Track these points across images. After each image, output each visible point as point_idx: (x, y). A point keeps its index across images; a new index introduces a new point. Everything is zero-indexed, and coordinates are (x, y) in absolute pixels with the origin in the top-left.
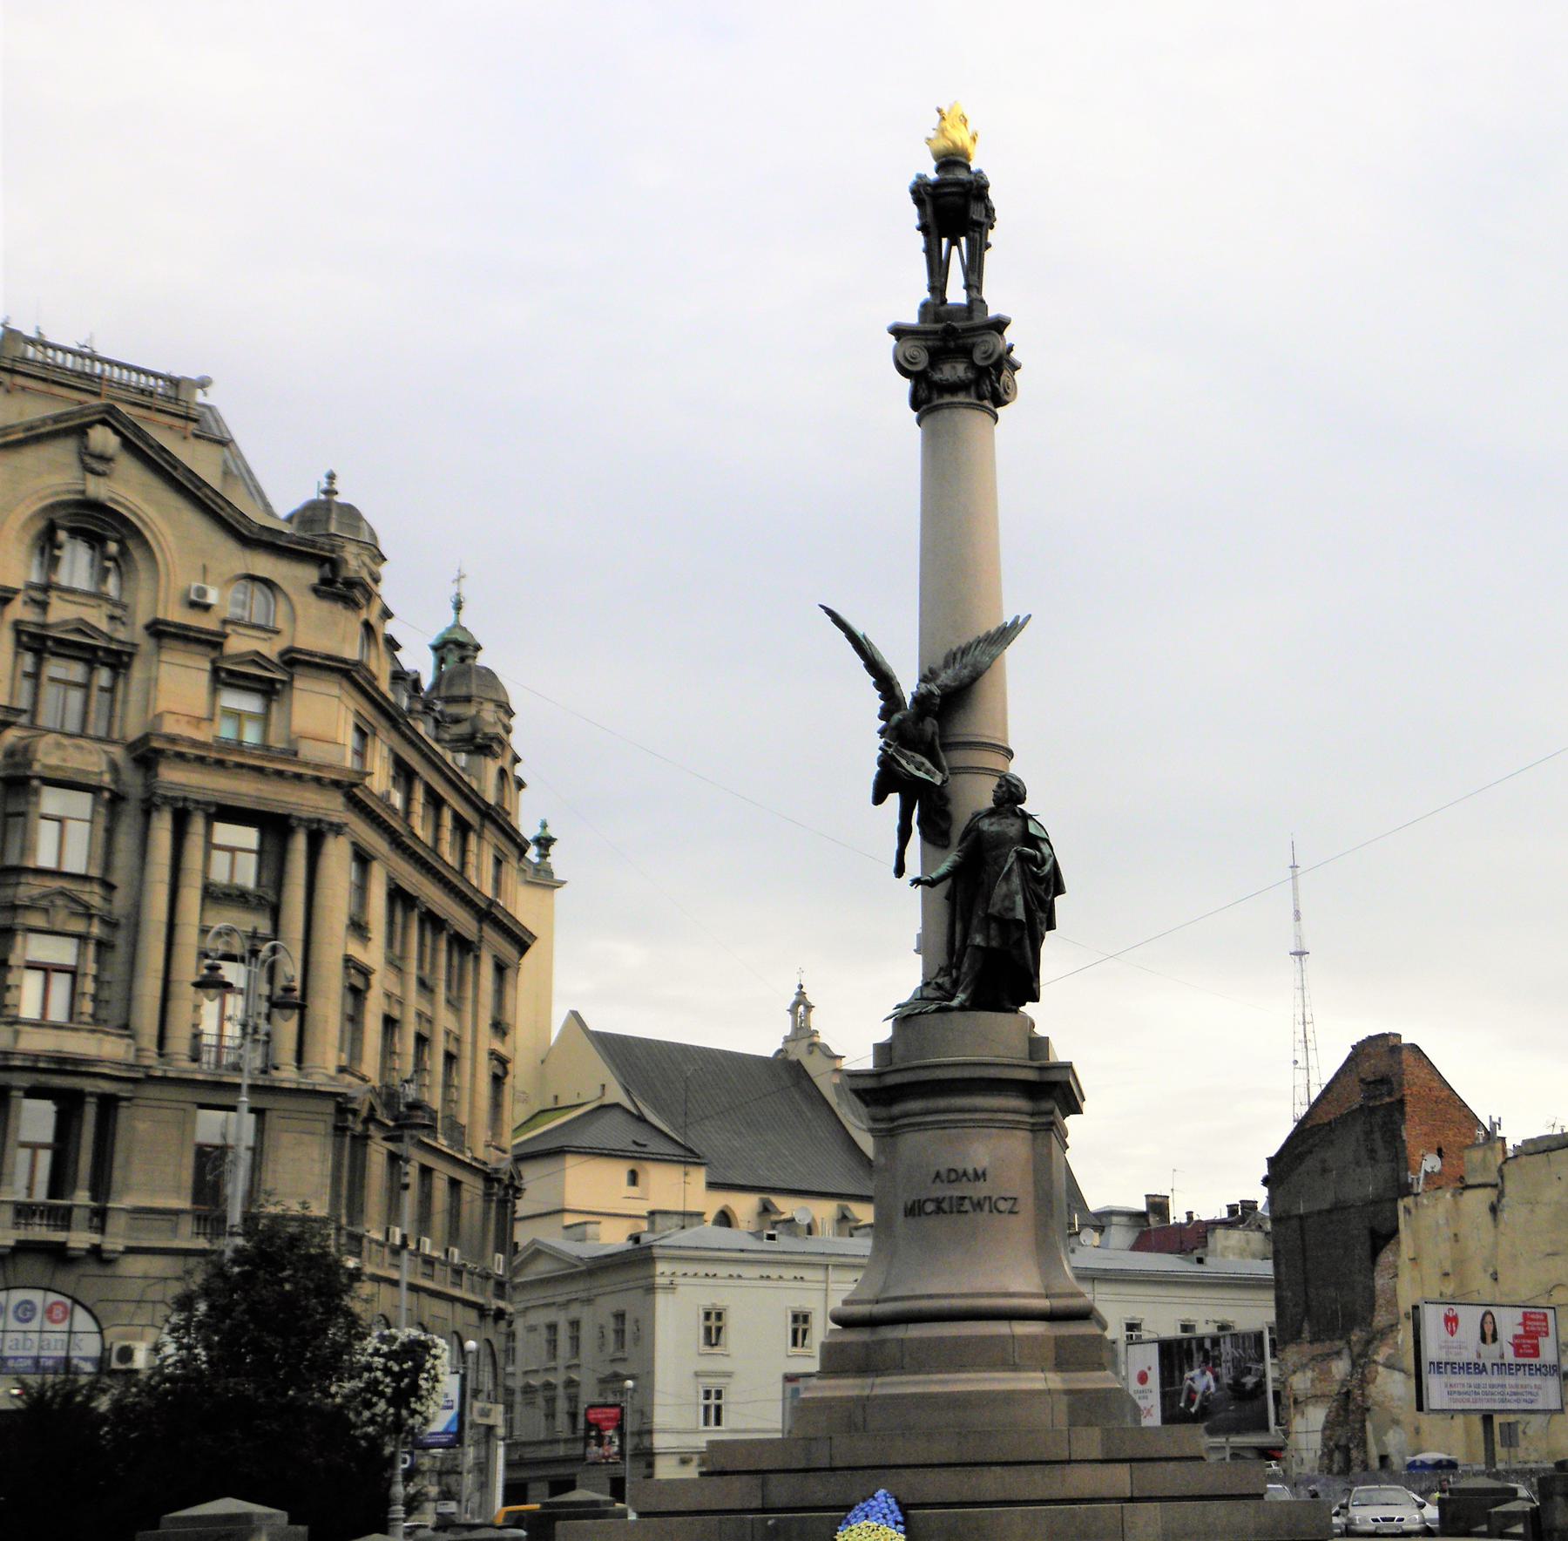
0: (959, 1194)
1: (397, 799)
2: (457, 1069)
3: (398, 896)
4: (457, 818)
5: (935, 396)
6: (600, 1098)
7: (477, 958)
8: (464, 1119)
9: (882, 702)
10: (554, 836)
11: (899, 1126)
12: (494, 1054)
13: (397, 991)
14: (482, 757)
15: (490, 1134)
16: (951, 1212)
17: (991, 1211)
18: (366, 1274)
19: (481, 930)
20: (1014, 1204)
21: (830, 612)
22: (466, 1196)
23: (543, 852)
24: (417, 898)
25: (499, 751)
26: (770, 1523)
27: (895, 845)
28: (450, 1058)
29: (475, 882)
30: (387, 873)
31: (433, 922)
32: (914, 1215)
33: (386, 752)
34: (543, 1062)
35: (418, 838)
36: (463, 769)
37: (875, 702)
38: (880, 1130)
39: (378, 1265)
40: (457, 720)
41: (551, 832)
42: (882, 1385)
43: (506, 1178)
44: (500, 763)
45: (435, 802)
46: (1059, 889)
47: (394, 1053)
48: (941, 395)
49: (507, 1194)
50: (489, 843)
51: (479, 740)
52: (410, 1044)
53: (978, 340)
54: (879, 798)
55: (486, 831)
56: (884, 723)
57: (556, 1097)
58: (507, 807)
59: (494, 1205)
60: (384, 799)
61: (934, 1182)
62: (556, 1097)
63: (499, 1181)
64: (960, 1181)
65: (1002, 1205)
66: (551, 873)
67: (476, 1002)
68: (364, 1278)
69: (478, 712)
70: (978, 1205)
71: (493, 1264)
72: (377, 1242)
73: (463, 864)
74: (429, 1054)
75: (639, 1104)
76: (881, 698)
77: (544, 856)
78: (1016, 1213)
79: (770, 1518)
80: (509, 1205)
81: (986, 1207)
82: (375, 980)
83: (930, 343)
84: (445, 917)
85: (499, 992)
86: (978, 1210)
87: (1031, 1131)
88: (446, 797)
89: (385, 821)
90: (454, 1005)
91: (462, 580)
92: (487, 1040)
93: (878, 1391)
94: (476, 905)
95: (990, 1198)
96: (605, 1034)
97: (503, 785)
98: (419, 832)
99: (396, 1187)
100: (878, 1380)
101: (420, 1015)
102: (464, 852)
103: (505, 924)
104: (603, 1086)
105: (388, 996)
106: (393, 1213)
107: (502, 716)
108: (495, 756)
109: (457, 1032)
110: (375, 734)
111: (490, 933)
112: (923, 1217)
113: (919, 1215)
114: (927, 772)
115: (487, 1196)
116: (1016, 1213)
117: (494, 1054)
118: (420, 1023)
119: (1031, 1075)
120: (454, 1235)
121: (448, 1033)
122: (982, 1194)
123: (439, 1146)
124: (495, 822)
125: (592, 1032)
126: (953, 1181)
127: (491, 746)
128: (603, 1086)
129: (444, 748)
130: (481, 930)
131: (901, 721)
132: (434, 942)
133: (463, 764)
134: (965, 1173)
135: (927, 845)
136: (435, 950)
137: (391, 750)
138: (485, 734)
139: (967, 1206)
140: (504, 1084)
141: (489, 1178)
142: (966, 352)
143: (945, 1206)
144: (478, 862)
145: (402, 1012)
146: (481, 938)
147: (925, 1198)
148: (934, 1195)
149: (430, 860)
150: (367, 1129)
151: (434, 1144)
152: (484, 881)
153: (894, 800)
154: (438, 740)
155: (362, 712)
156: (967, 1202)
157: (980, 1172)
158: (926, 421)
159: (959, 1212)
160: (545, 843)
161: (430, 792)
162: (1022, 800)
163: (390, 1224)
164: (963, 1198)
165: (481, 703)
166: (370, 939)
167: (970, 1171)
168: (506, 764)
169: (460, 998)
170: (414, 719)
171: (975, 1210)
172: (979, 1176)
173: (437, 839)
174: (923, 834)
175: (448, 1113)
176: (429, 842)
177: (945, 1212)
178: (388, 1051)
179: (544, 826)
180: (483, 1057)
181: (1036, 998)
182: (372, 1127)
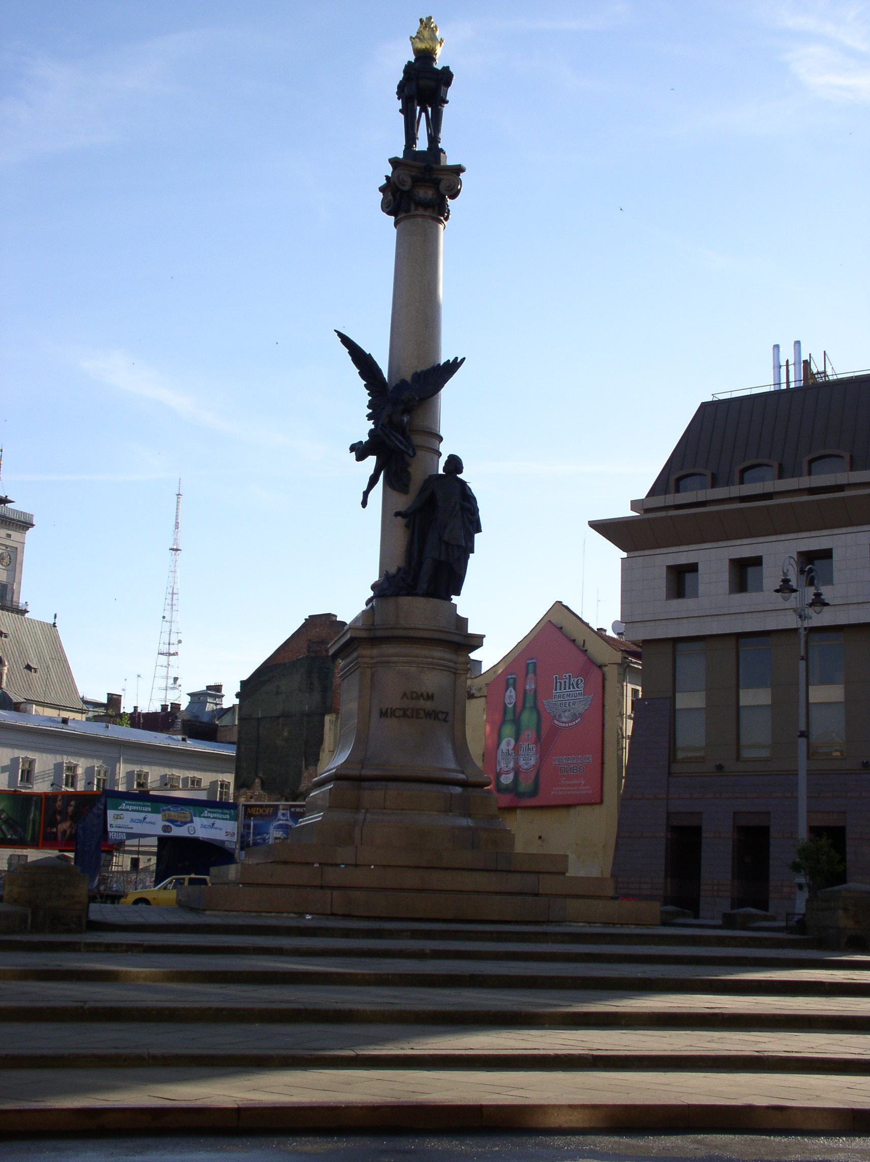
5: (413, 207)
9: (370, 398)
16: (412, 717)
20: (446, 717)
21: (340, 335)
27: (365, 489)
32: (387, 717)
37: (364, 397)
46: (479, 530)
48: (416, 209)
53: (445, 177)
54: (360, 457)
56: (371, 411)
61: (402, 698)
64: (419, 699)
65: (441, 716)
78: (447, 721)
83: (414, 174)
87: (455, 673)
113: (391, 717)
114: (406, 447)
116: (447, 721)
126: (415, 699)
135: (389, 489)
142: (436, 183)
143: (409, 713)
147: (394, 708)
153: (371, 461)
157: (430, 695)
158: (402, 224)
159: (417, 718)
162: (461, 472)
171: (426, 718)
172: (430, 697)
177: (408, 717)
181: (458, 594)
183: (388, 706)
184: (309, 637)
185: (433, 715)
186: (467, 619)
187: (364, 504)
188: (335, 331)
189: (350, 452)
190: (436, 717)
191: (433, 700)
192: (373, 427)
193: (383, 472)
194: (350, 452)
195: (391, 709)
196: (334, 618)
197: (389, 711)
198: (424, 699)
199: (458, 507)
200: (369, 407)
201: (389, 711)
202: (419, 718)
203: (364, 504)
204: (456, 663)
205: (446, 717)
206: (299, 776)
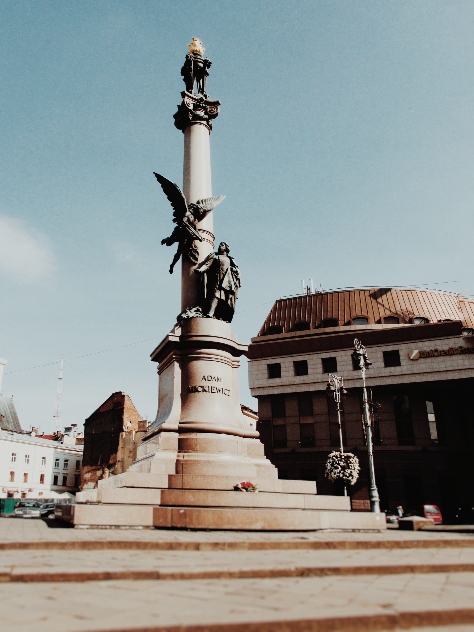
16: (209, 392)
20: (229, 393)
26: (181, 511)
37: (171, 210)
42: (188, 456)
70: (218, 391)
76: (174, 209)
79: (182, 509)
81: (221, 392)
86: (218, 391)
93: (185, 458)
100: (186, 454)
143: (207, 389)
148: (202, 385)
157: (219, 378)
159: (212, 392)
164: (214, 387)
171: (218, 392)
177: (206, 392)
184: (114, 401)
185: (221, 392)
187: (171, 272)
188: (154, 173)
189: (162, 244)
192: (177, 225)
193: (181, 255)
194: (162, 244)
196: (123, 394)
199: (229, 270)
200: (174, 215)
203: (171, 272)
205: (229, 393)
206: (109, 459)
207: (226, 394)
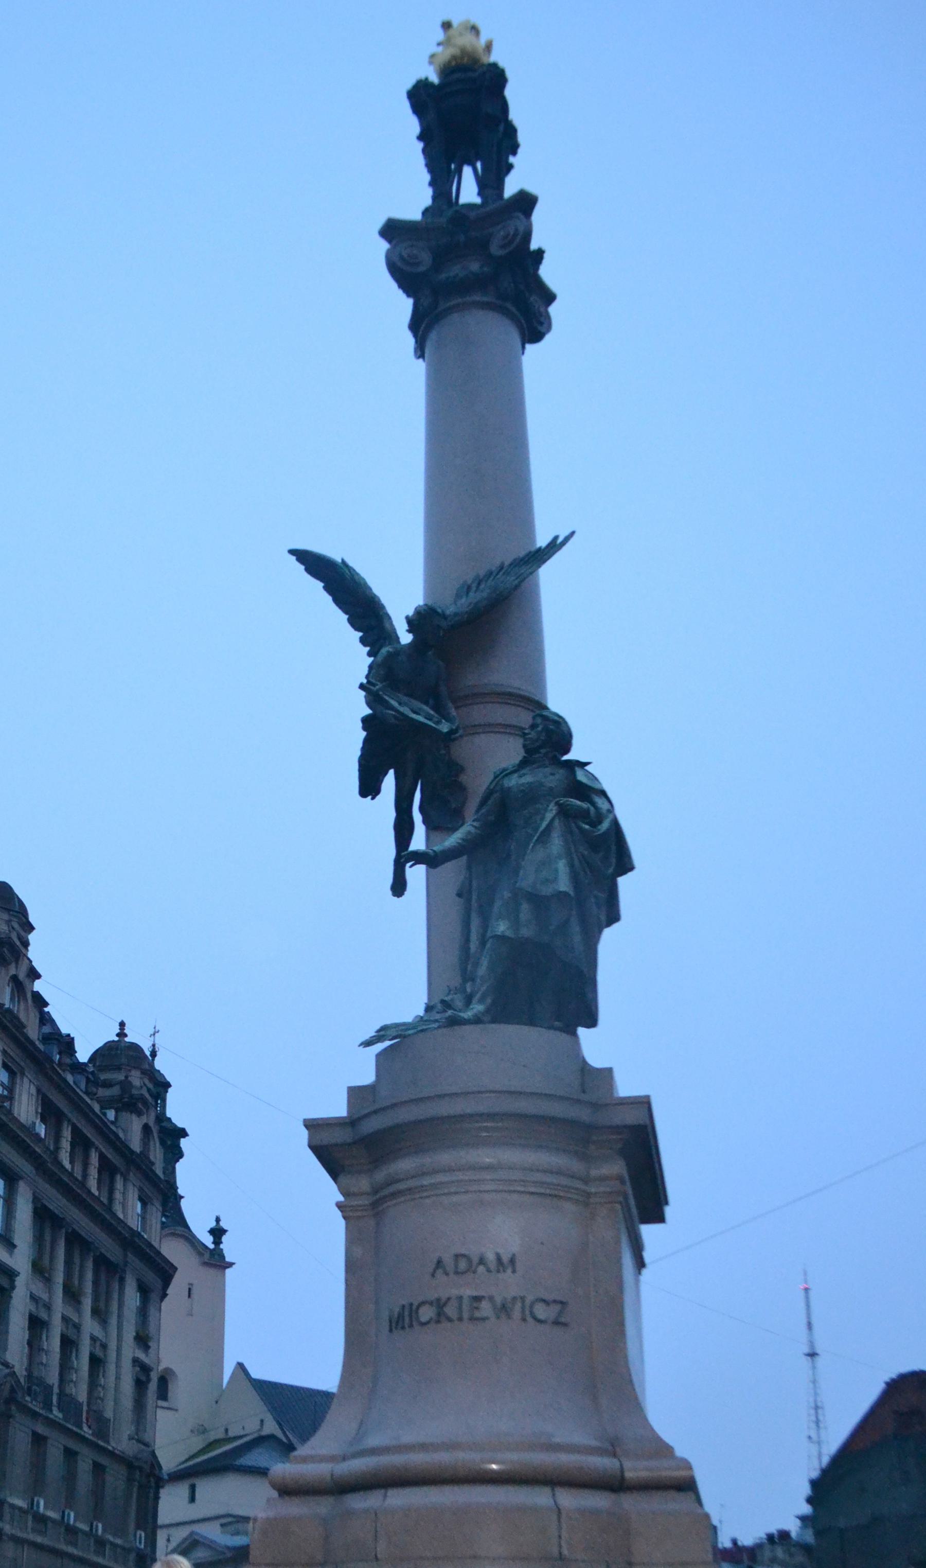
0: (468, 1292)
1: (41, 1130)
2: (104, 1371)
3: (42, 1214)
4: (102, 1157)
6: (260, 1430)
7: (122, 1280)
8: (109, 1414)
10: (225, 1228)
11: (385, 1197)
12: (136, 1361)
13: (45, 1297)
14: (129, 1113)
15: (133, 1428)
16: (460, 1319)
17: (524, 1320)
18: (7, 1535)
19: (126, 1256)
22: (109, 1479)
23: (217, 1240)
24: (63, 1219)
25: (145, 1111)
28: (96, 1362)
29: (121, 1216)
30: (34, 1194)
31: (76, 1241)
32: (403, 1328)
33: (33, 1090)
34: (217, 1402)
35: (63, 1167)
36: (112, 1122)
38: (354, 1208)
39: (21, 1529)
40: (107, 1084)
41: (223, 1224)
43: (147, 1468)
44: (144, 1119)
45: (81, 1143)
47: (43, 1349)
49: (149, 1482)
50: (134, 1184)
51: (126, 1100)
52: (56, 1343)
55: (131, 1174)
57: (227, 1430)
58: (152, 1158)
59: (135, 1489)
60: (30, 1130)
62: (227, 1430)
63: (141, 1469)
65: (541, 1311)
66: (223, 1257)
67: (120, 1316)
68: (4, 1537)
69: (126, 1077)
71: (135, 1539)
72: (20, 1509)
73: (111, 1199)
74: (77, 1356)
75: (290, 1436)
77: (217, 1241)
80: (151, 1491)
81: (517, 1313)
82: (20, 1281)
84: (90, 1240)
85: (143, 1312)
86: (503, 1316)
88: (93, 1140)
89: (29, 1146)
90: (100, 1314)
91: (156, 1034)
92: (130, 1350)
94: (120, 1233)
95: (523, 1299)
96: (265, 1382)
97: (149, 1140)
98: (68, 1166)
99: (38, 1466)
101: (65, 1319)
102: (111, 1191)
103: (147, 1253)
104: (262, 1421)
105: (34, 1298)
106: (37, 1486)
107: (147, 1081)
108: (139, 1114)
109: (104, 1341)
110: (23, 1074)
111: (131, 1257)
112: (417, 1327)
115: (130, 1480)
117: (136, 1361)
118: (67, 1328)
119: (584, 1115)
120: (97, 1512)
121: (93, 1339)
122: (513, 1292)
123: (83, 1433)
124: (139, 1168)
125: (255, 1380)
126: (463, 1273)
127: (135, 1104)
128: (262, 1421)
129: (91, 1099)
130: (126, 1256)
131: (390, 655)
132: (82, 1260)
133: (113, 1119)
134: (482, 1261)
136: (82, 1267)
137: (39, 1091)
138: (132, 1096)
139: (486, 1308)
140: (147, 1388)
141: (129, 1464)
143: (451, 1310)
144: (124, 1199)
145: (49, 1316)
146: (126, 1263)
147: (416, 1304)
148: (432, 1295)
149: (74, 1187)
150: (10, 1409)
151: (79, 1431)
152: (130, 1217)
154: (87, 1093)
155: (9, 1051)
156: (485, 1305)
157: (505, 1259)
159: (472, 1319)
160: (218, 1233)
161: (76, 1131)
163: (36, 1495)
164: (477, 1299)
165: (130, 1071)
166: (14, 1246)
167: (491, 1257)
168: (151, 1124)
169: (107, 1312)
170: (64, 1071)
171: (498, 1318)
172: (506, 1264)
173: (85, 1175)
174: (425, 821)
175: (95, 1408)
176: (78, 1174)
178: (34, 1345)
179: (218, 1220)
180: (127, 1364)
182: (13, 1408)
183: (404, 1303)
185: (517, 1313)
186: (609, 1071)
190: (529, 1315)
191: (514, 1271)
195: (411, 1305)
197: (406, 1313)
198: (489, 1271)
201: (406, 1313)
202: (477, 1319)
204: (586, 1180)
207: (541, 1315)
